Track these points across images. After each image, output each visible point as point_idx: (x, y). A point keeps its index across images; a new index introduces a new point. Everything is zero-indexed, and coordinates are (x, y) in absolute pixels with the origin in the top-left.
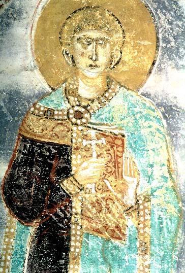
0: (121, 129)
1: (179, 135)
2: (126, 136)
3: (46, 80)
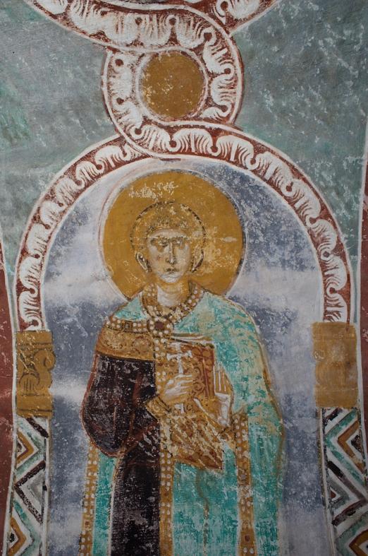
0: (208, 339)
1: (275, 342)
2: (215, 345)
3: (121, 289)
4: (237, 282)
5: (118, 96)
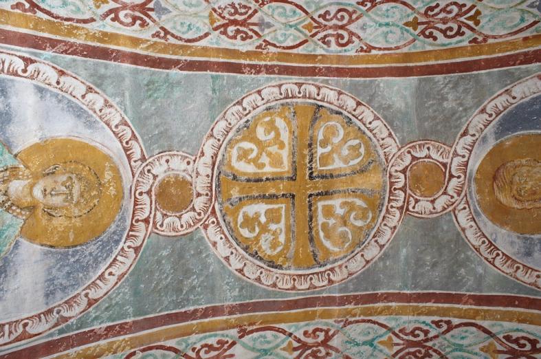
4: (35, 246)
5: (170, 160)
